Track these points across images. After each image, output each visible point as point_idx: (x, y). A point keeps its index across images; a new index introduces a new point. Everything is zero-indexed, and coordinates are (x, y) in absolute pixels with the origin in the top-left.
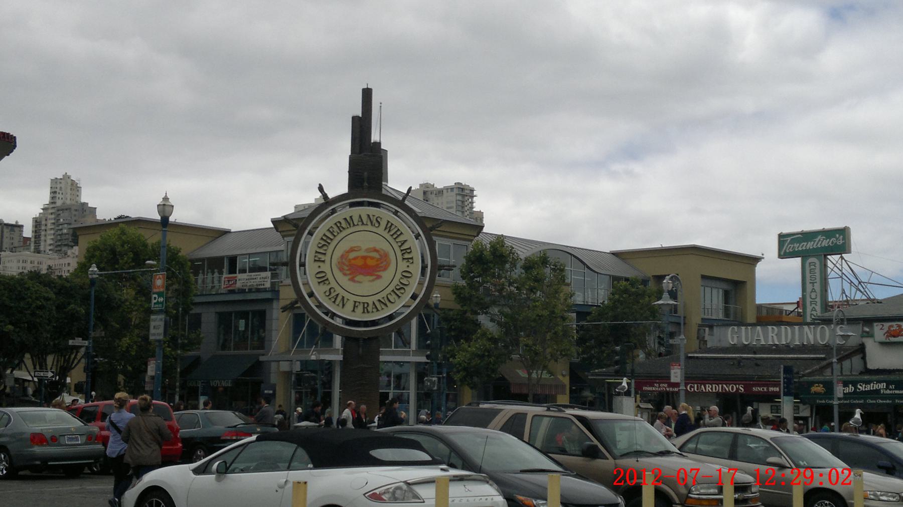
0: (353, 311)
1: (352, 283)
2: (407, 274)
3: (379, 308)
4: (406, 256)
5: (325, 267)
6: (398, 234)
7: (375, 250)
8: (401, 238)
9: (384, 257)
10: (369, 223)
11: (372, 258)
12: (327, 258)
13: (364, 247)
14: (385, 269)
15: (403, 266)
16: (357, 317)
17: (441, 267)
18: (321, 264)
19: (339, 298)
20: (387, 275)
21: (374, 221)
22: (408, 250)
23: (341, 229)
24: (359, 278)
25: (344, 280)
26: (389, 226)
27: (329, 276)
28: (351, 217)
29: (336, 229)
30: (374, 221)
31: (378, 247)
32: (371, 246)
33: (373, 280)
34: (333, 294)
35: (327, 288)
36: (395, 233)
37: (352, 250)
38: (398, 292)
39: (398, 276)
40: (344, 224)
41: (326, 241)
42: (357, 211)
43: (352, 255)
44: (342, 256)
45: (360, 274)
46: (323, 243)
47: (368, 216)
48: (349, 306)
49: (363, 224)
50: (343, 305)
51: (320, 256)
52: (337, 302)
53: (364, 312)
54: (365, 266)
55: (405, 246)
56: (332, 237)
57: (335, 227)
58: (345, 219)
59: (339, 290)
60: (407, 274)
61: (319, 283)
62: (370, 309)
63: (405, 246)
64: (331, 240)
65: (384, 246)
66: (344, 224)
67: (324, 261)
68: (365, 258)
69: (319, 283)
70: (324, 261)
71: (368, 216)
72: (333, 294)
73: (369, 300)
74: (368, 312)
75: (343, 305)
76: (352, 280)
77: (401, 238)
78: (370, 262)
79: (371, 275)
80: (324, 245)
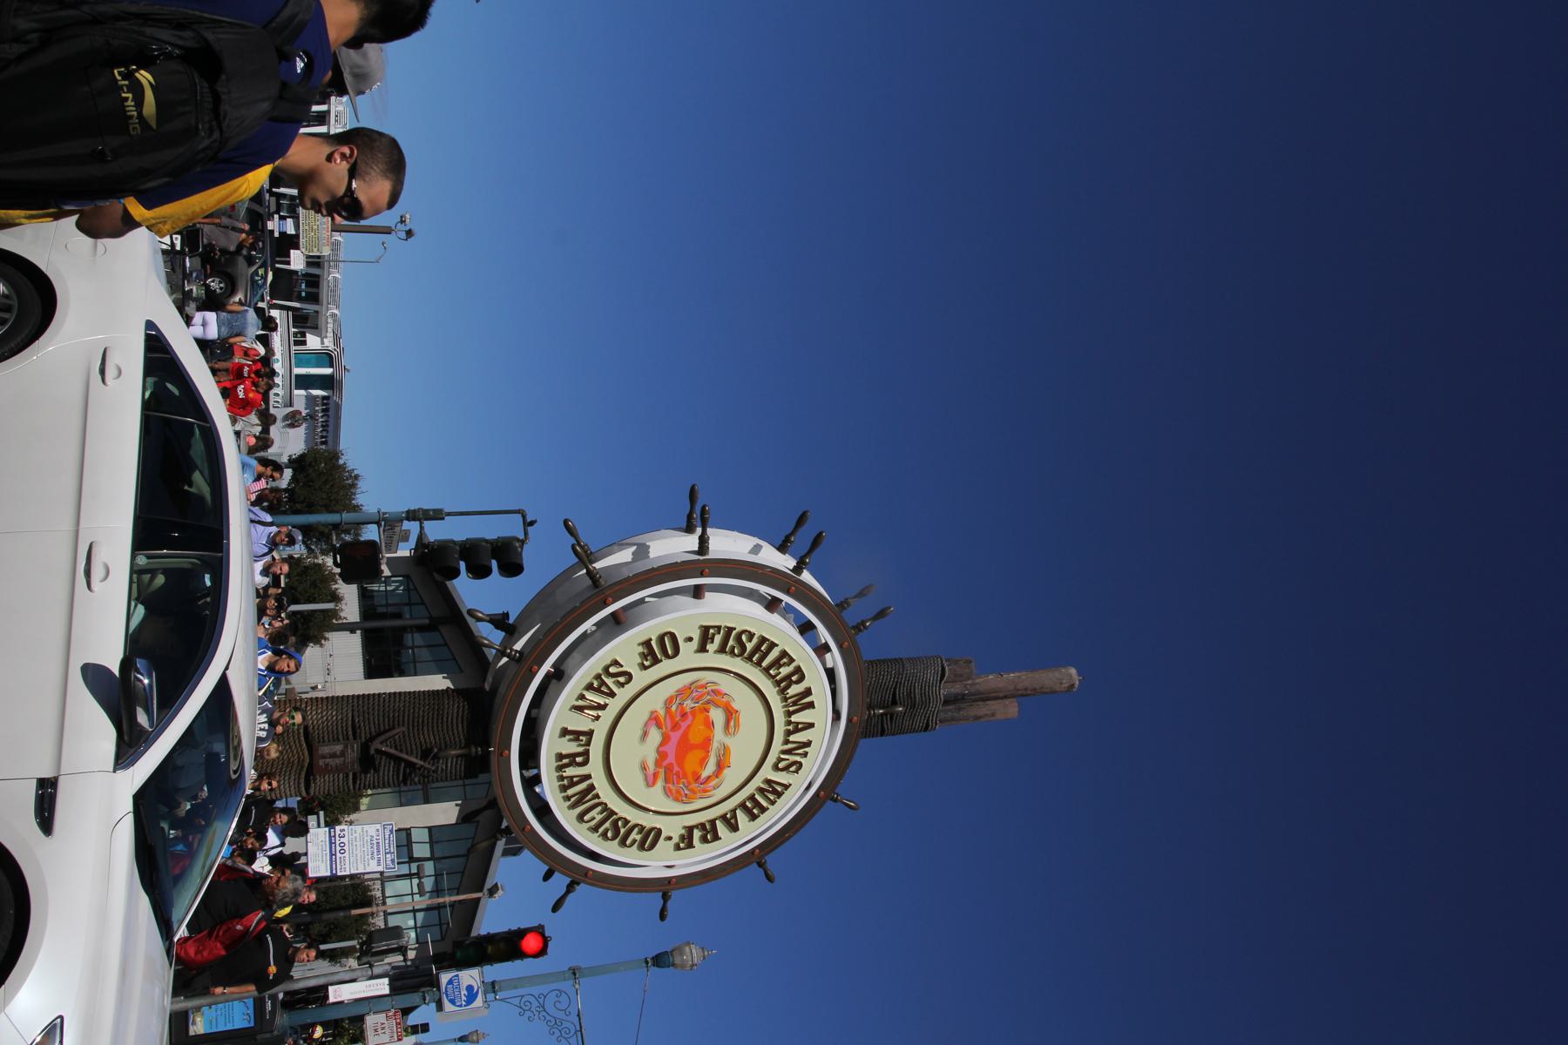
0: (565, 732)
1: (646, 717)
2: (650, 838)
3: (570, 792)
4: (697, 834)
5: (688, 655)
6: (753, 809)
7: (720, 766)
8: (741, 817)
9: (700, 784)
10: (790, 746)
11: (703, 762)
12: (712, 658)
13: (728, 741)
14: (667, 792)
15: (672, 828)
16: (551, 745)
17: (666, 897)
18: (695, 644)
19: (601, 700)
20: (655, 797)
21: (793, 758)
22: (710, 833)
23: (783, 684)
24: (655, 736)
25: (654, 701)
26: (774, 791)
27: (666, 666)
28: (811, 705)
29: (785, 671)
30: (793, 758)
31: (726, 771)
32: (733, 759)
33: (644, 768)
34: (609, 681)
35: (630, 663)
36: (757, 804)
37: (730, 714)
38: (607, 825)
39: (648, 821)
40: (794, 690)
41: (759, 650)
42: (821, 714)
43: (717, 715)
44: (716, 692)
45: (666, 739)
46: (749, 646)
47: (808, 744)
48: (580, 723)
49: (789, 733)
50: (580, 709)
51: (718, 639)
52: (590, 696)
53: (560, 757)
54: (683, 750)
55: (721, 828)
56: (764, 664)
57: (790, 669)
58: (808, 692)
59: (623, 695)
60: (650, 838)
61: (647, 644)
62: (570, 771)
63: (721, 828)
64: (759, 664)
65: (732, 778)
66: (794, 690)
67: (702, 649)
68: (706, 744)
69: (647, 644)
70: (702, 649)
71: (808, 744)
72: (609, 681)
73: (595, 768)
74: (560, 768)
75: (580, 709)
76: (654, 719)
77: (741, 817)
78: (692, 759)
79: (658, 763)
80: (743, 648)
